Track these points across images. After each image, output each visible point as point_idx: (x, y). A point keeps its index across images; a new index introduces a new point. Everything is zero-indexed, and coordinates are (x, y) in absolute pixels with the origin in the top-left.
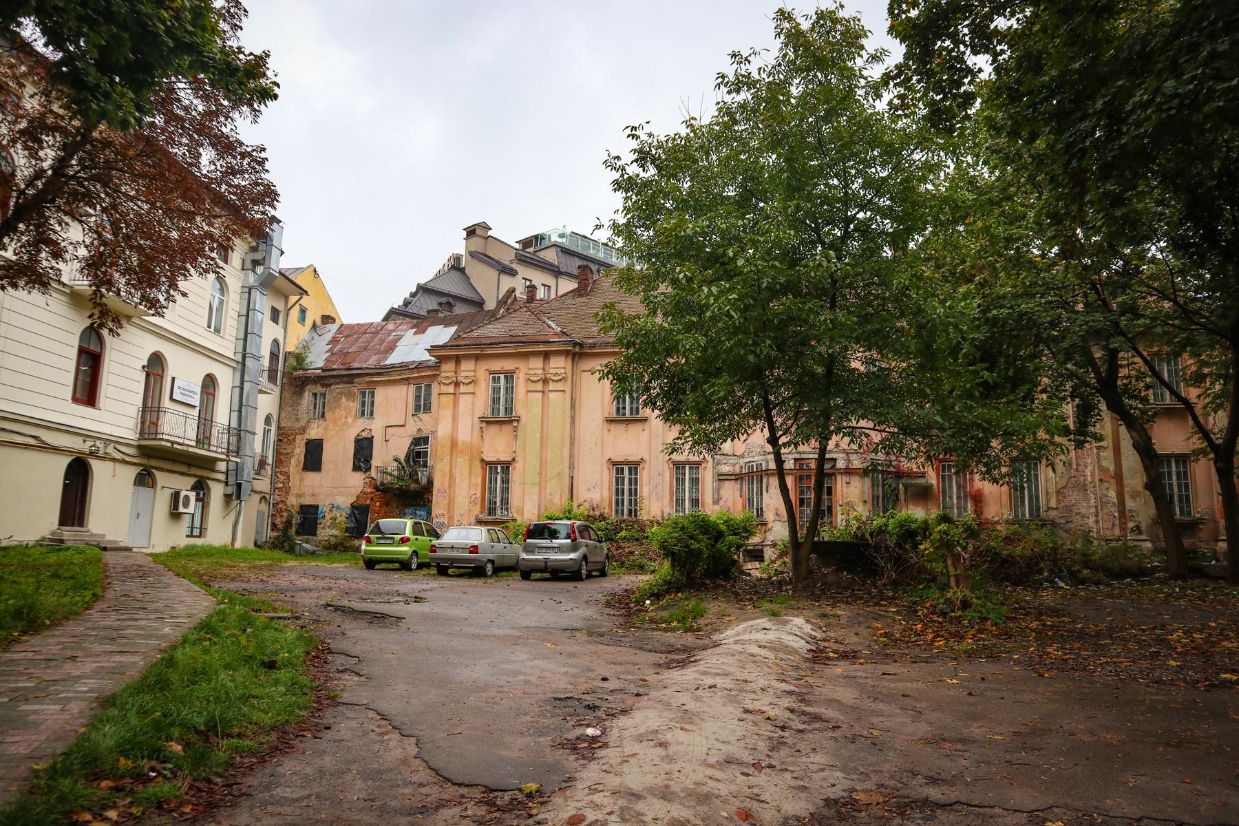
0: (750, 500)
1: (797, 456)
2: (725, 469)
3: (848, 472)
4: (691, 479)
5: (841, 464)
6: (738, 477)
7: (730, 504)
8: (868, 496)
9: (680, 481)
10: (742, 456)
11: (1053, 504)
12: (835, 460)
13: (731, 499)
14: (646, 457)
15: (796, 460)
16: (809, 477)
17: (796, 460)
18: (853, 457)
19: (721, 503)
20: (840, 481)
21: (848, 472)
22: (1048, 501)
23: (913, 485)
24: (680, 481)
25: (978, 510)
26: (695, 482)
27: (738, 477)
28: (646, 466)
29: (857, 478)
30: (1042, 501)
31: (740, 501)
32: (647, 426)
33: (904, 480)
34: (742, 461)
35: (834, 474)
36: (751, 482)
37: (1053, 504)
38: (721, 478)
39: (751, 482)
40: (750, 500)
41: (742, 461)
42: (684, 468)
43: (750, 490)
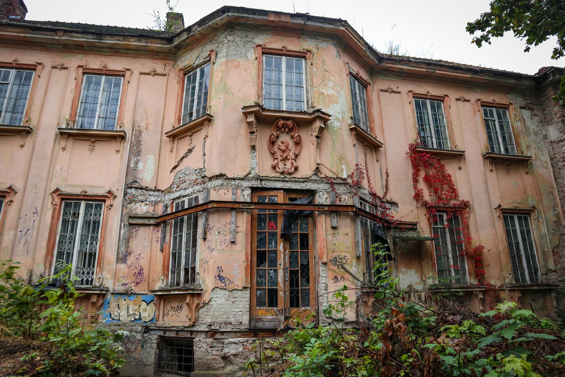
0: (176, 256)
1: (257, 184)
2: (141, 209)
3: (335, 210)
4: (87, 223)
5: (322, 198)
6: (160, 222)
7: (144, 263)
8: (361, 250)
9: (69, 225)
10: (169, 191)
11: (551, 266)
12: (312, 193)
13: (146, 254)
14: (18, 186)
15: (254, 190)
16: (274, 217)
17: (254, 190)
18: (341, 189)
19: (131, 260)
20: (323, 224)
21: (335, 210)
22: (546, 261)
23: (403, 240)
24: (69, 225)
25: (479, 273)
26: (93, 226)
27: (160, 222)
28: (17, 199)
29: (348, 221)
30: (539, 262)
31: (159, 257)
32: (29, 142)
33: (392, 232)
34: (168, 198)
35: (311, 214)
36: (179, 226)
37: (551, 266)
38: (134, 222)
39: (179, 226)
40: (176, 256)
41: (168, 198)
42: (78, 206)
43: (177, 241)
